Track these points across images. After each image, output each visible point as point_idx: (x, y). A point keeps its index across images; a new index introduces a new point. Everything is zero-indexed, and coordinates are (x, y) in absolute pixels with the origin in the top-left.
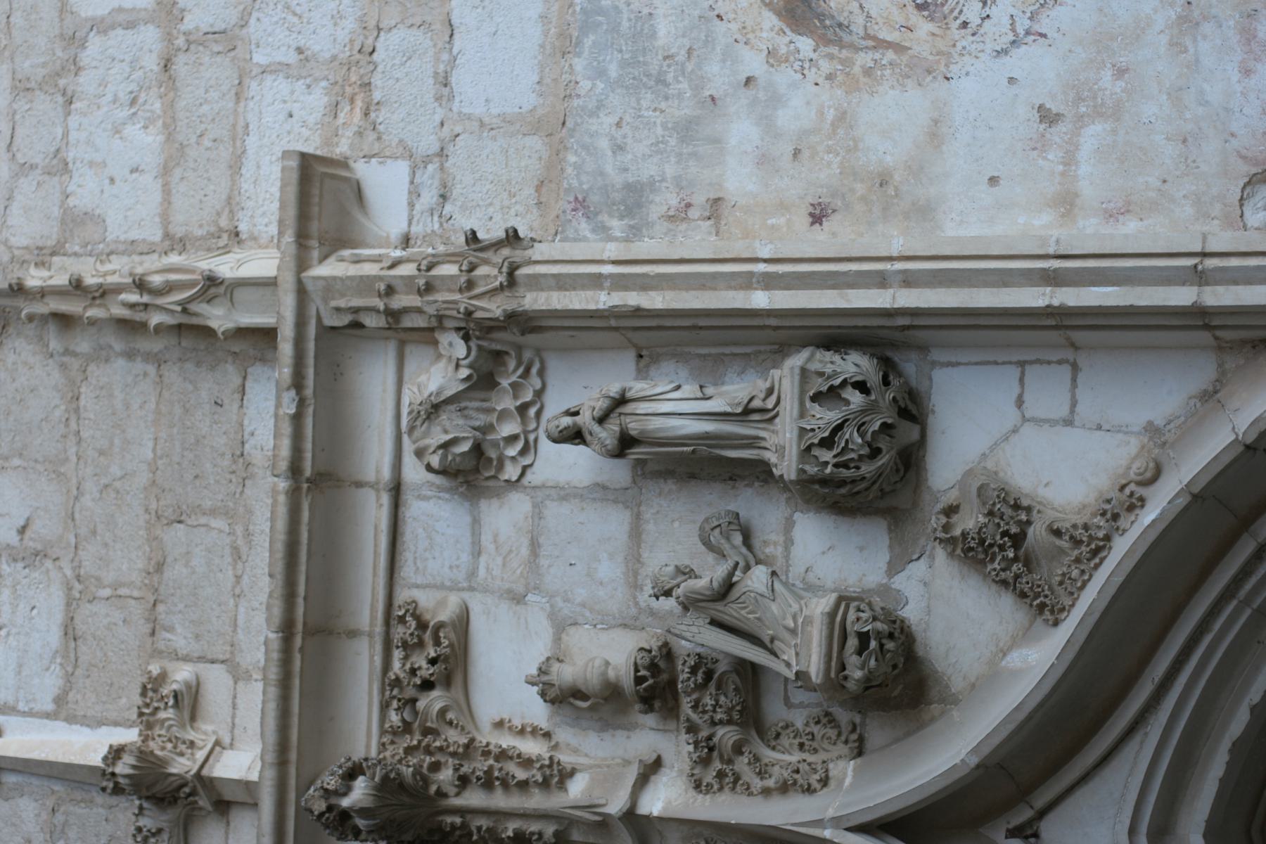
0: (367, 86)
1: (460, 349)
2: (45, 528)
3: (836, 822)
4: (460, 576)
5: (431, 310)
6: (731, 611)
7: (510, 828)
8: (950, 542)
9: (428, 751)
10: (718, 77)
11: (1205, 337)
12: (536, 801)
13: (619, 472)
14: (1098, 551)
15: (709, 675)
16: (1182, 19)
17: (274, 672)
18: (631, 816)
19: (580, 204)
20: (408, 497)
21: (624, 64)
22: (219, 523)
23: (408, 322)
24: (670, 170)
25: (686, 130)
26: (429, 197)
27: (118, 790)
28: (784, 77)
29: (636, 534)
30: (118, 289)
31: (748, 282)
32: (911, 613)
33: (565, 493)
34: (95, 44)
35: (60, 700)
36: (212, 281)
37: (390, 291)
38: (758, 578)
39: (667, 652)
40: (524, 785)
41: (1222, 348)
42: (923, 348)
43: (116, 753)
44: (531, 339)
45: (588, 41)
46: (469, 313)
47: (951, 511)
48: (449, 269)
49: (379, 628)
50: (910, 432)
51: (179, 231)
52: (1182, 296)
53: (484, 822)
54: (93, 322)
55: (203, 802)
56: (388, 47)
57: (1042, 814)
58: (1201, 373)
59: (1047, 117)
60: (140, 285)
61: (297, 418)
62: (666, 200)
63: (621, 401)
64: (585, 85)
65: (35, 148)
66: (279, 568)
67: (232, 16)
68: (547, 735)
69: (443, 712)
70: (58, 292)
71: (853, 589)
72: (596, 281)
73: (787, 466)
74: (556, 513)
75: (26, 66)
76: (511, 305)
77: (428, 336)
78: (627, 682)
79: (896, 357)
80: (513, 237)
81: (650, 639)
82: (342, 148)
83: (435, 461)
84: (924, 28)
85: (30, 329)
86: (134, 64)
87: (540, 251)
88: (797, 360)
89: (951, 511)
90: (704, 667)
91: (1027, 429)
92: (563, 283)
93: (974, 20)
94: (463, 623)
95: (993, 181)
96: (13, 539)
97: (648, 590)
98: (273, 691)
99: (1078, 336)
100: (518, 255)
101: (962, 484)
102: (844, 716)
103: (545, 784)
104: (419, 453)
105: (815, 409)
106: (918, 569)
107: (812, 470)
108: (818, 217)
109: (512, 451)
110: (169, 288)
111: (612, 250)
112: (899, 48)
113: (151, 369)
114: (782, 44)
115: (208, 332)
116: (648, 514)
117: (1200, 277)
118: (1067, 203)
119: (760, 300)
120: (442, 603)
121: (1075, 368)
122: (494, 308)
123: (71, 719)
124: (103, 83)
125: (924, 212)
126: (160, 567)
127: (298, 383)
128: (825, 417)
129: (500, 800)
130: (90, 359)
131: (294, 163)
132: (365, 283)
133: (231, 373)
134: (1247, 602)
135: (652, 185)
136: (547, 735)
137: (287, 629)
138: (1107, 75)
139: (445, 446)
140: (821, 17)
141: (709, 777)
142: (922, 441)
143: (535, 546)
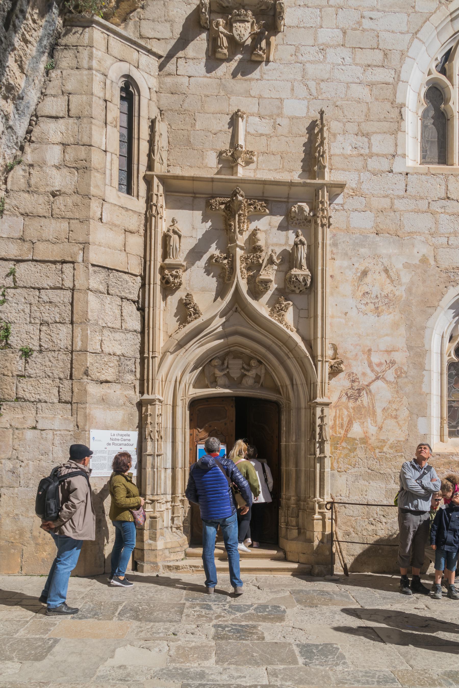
2: (279, 129)
3: (238, 280)
14: (281, 322)
22: (281, 166)
51: (332, 158)
52: (319, 335)
62: (335, 251)
75: (363, 125)
93: (362, 302)
96: (277, 123)
97: (273, 248)
105: (302, 278)
114: (359, 270)
119: (320, 268)
122: (319, 221)
126: (274, 154)
128: (301, 279)
132: (323, 197)
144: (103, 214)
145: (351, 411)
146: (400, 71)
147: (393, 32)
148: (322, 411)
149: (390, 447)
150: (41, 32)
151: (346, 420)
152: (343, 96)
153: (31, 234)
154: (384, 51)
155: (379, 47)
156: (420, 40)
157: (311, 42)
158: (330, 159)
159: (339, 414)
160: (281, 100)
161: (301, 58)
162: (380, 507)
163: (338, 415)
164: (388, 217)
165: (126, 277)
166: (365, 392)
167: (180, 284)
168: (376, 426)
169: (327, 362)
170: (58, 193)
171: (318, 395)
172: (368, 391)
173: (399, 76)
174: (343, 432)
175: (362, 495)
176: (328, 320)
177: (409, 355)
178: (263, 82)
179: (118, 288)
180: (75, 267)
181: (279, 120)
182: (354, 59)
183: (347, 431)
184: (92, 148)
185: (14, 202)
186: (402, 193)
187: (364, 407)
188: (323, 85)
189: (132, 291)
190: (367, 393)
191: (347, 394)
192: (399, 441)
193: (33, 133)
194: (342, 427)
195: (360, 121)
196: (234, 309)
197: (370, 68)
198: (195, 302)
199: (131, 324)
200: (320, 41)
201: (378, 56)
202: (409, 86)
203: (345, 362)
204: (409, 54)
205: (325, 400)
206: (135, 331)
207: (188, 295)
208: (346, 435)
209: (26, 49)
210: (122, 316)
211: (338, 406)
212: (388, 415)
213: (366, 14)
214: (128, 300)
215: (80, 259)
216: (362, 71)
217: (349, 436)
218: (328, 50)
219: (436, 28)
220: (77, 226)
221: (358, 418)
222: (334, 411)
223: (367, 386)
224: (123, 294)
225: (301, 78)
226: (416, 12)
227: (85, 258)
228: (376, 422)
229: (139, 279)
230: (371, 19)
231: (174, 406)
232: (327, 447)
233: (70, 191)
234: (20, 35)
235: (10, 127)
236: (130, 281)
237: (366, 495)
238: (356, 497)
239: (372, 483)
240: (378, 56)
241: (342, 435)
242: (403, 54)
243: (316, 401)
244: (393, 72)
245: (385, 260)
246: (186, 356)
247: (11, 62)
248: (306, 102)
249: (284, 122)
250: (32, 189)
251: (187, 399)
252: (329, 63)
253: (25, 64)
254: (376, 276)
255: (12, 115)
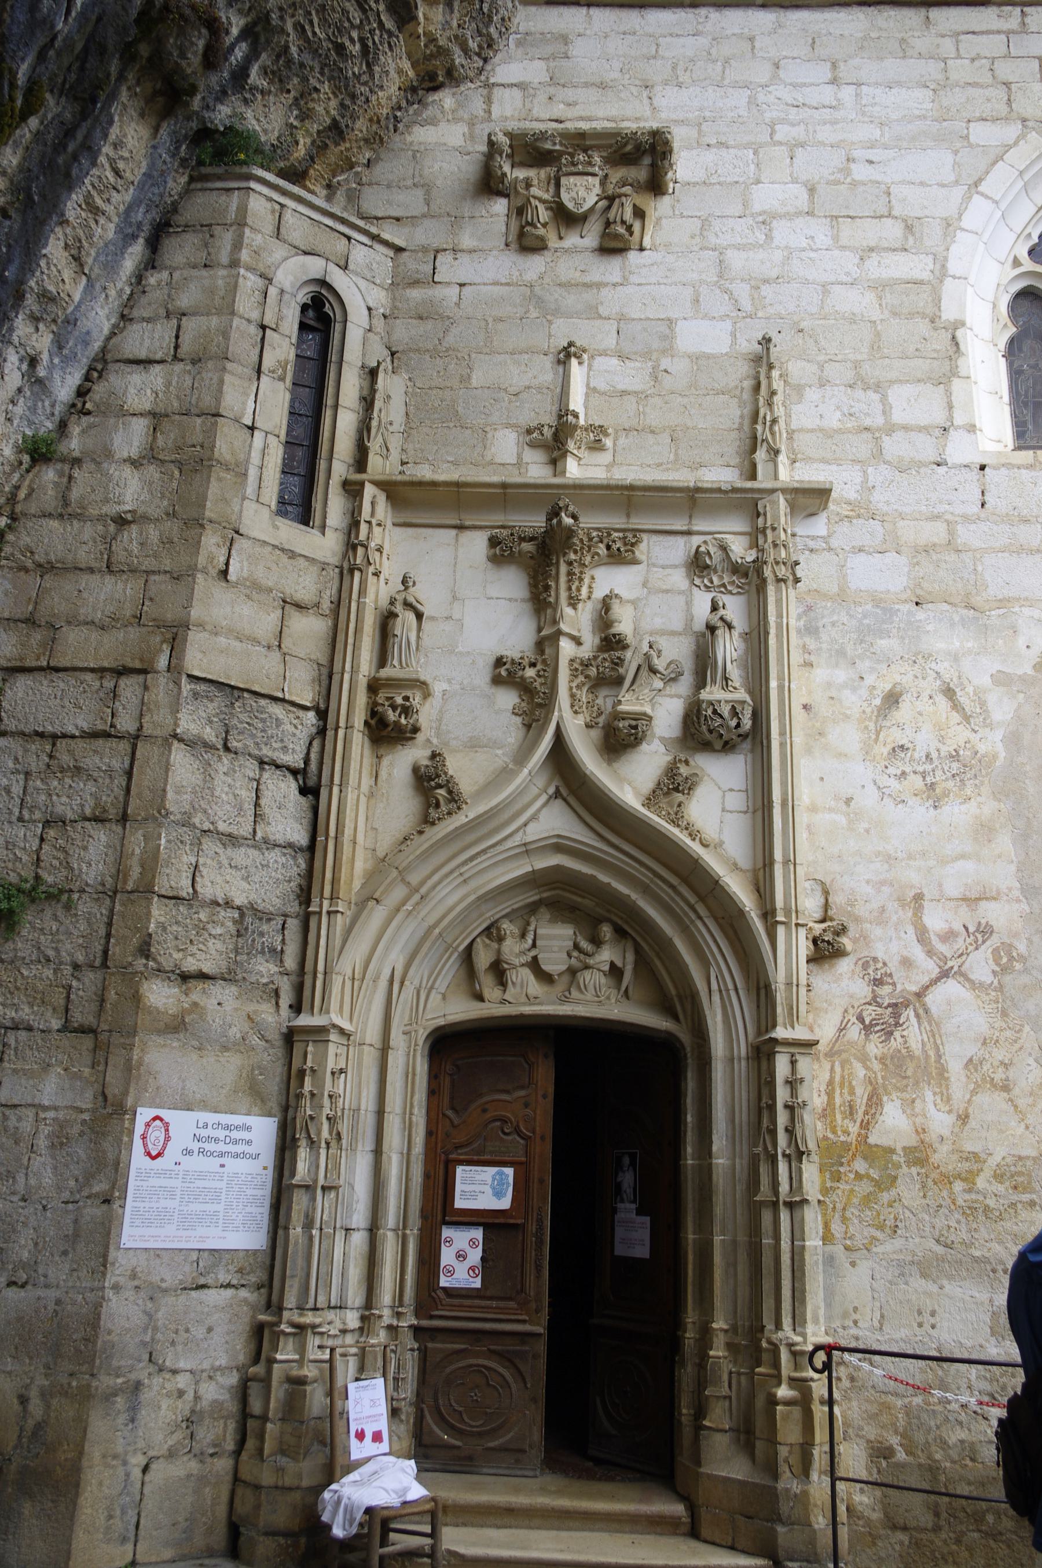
0: (859, 516)
1: (749, 559)
2: (667, 381)
3: (561, 717)
4: (653, 560)
5: (766, 546)
6: (644, 673)
7: (552, 584)
8: (675, 763)
9: (582, 548)
10: (864, 665)
11: (760, 865)
12: (563, 595)
13: (699, 625)
14: (675, 823)
15: (617, 664)
16: (889, 856)
17: (613, 482)
18: (559, 633)
19: (810, 608)
20: (685, 538)
21: (868, 625)
22: (672, 456)
23: (760, 536)
24: (824, 646)
25: (841, 653)
26: (811, 544)
27: (560, 417)
28: (864, 693)
29: (673, 633)
30: (771, 410)
31: (780, 679)
32: (644, 747)
33: (689, 604)
34: (875, 397)
35: (595, 390)
36: (777, 452)
37: (774, 529)
38: (658, 684)
39: (625, 647)
40: (570, 589)
41: (755, 871)
42: (752, 751)
43: (576, 416)
44: (754, 589)
45: (878, 611)
46: (765, 563)
47: (687, 762)
48: (783, 555)
49: (631, 526)
50: (718, 745)
51: (795, 436)
52: (778, 855)
53: (553, 572)
54: (757, 401)
55: (556, 454)
56: (875, 525)
57: (565, 800)
58: (744, 861)
59: (848, 801)
60: (774, 421)
61: (719, 490)
63: (730, 627)
64: (860, 610)
65: (832, 371)
66: (657, 484)
67: (888, 458)
68: (589, 598)
69: (598, 554)
70: (770, 385)
71: (654, 722)
72: (780, 616)
73: (705, 695)
74: (681, 600)
76: (769, 581)
77: (754, 545)
78: (613, 631)
79: (749, 740)
80: (797, 580)
81: (630, 640)
82: (831, 506)
83: (702, 549)
84: (885, 751)
85: (752, 372)
86: (867, 414)
87: (792, 593)
88: (748, 699)
89: (687, 762)
90: (619, 662)
91: (720, 793)
92: (779, 602)
93: (888, 771)
94: (635, 562)
95: (822, 779)
96: (662, 368)
98: (605, 482)
99: (759, 814)
100: (790, 583)
101: (697, 767)
102: (601, 720)
103: (570, 598)
104: (705, 542)
105: (729, 707)
106: (662, 749)
107: (704, 706)
108: (805, 707)
109: (706, 581)
110: (773, 433)
111: (792, 622)
112: (876, 740)
113: (736, 426)
114: (878, 692)
115: (754, 450)
116: (682, 638)
117: (786, 862)
118: (813, 809)
119: (773, 684)
120: (642, 553)
121: (746, 812)
122: (768, 572)
123: (587, 395)
124: (859, 401)
125: (809, 751)
126: (653, 432)
127: (735, 490)
128: (725, 710)
129: (563, 579)
130: (740, 398)
131: (827, 486)
132: (777, 518)
133: (735, 461)
134: (652, 881)
135: (818, 638)
136: (589, 598)
137: (631, 488)
138: (866, 826)
139: (709, 553)
140: (889, 708)
141: (576, 665)
142: (714, 751)
143: (667, 591)
144: (231, 561)
145: (876, 1066)
146: (946, 259)
147: (922, 184)
148: (793, 1063)
149: (995, 1176)
150: (128, 196)
151: (861, 1094)
152: (814, 310)
153: (56, 604)
154: (905, 221)
155: (893, 213)
156: (987, 197)
157: (736, 209)
158: (790, 438)
159: (843, 1077)
160: (670, 322)
161: (713, 240)
162: (980, 1367)
163: (837, 1079)
164: (943, 565)
165: (277, 710)
166: (912, 1014)
167: (416, 730)
168: (950, 1112)
169: (803, 925)
170: (129, 517)
171: (780, 1020)
172: (921, 1011)
173: (943, 266)
174: (854, 1129)
175: (920, 1325)
176: (802, 818)
177: (1027, 909)
178: (629, 290)
179: (253, 736)
180: (149, 681)
181: (665, 363)
182: (836, 238)
183: (865, 1126)
184: (219, 419)
185: (26, 540)
186: (976, 508)
187: (912, 1057)
188: (766, 290)
189: (291, 746)
190: (917, 1016)
191: (861, 1019)
192: (1020, 1158)
193: (91, 394)
194: (851, 1114)
195: (859, 357)
196: (551, 790)
197: (874, 254)
198: (450, 772)
199: (280, 828)
200: (757, 207)
201: (892, 231)
202: (970, 290)
203: (852, 932)
204: (964, 224)
205: (799, 1033)
206: (290, 845)
207: (434, 756)
208: (863, 1139)
209: (93, 226)
210: (257, 805)
211: (839, 1052)
212: (984, 1080)
213: (857, 154)
214: (278, 767)
215: (162, 662)
216: (857, 261)
217: (872, 1140)
218: (775, 224)
219: (1021, 173)
220: (163, 587)
221: (898, 1089)
222: (827, 1066)
223: (920, 995)
224: (266, 752)
225: (715, 279)
226: (971, 146)
227: (174, 661)
228: (949, 1099)
229: (311, 717)
230: (871, 162)
231: (385, 1049)
232: (811, 1173)
233: (153, 512)
234: (81, 197)
235: (40, 381)
236: (286, 720)
237: (933, 1327)
238: (903, 1333)
239: (948, 1287)
240: (892, 231)
241: (852, 1138)
242: (950, 226)
243: (773, 1035)
244: (930, 259)
245: (945, 668)
246: (423, 913)
247: (54, 249)
248: (728, 325)
249: (678, 366)
250: (70, 510)
251: (421, 1031)
252: (778, 247)
253: (88, 254)
254: (923, 705)
255: (45, 357)
